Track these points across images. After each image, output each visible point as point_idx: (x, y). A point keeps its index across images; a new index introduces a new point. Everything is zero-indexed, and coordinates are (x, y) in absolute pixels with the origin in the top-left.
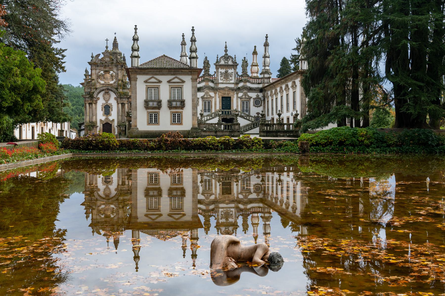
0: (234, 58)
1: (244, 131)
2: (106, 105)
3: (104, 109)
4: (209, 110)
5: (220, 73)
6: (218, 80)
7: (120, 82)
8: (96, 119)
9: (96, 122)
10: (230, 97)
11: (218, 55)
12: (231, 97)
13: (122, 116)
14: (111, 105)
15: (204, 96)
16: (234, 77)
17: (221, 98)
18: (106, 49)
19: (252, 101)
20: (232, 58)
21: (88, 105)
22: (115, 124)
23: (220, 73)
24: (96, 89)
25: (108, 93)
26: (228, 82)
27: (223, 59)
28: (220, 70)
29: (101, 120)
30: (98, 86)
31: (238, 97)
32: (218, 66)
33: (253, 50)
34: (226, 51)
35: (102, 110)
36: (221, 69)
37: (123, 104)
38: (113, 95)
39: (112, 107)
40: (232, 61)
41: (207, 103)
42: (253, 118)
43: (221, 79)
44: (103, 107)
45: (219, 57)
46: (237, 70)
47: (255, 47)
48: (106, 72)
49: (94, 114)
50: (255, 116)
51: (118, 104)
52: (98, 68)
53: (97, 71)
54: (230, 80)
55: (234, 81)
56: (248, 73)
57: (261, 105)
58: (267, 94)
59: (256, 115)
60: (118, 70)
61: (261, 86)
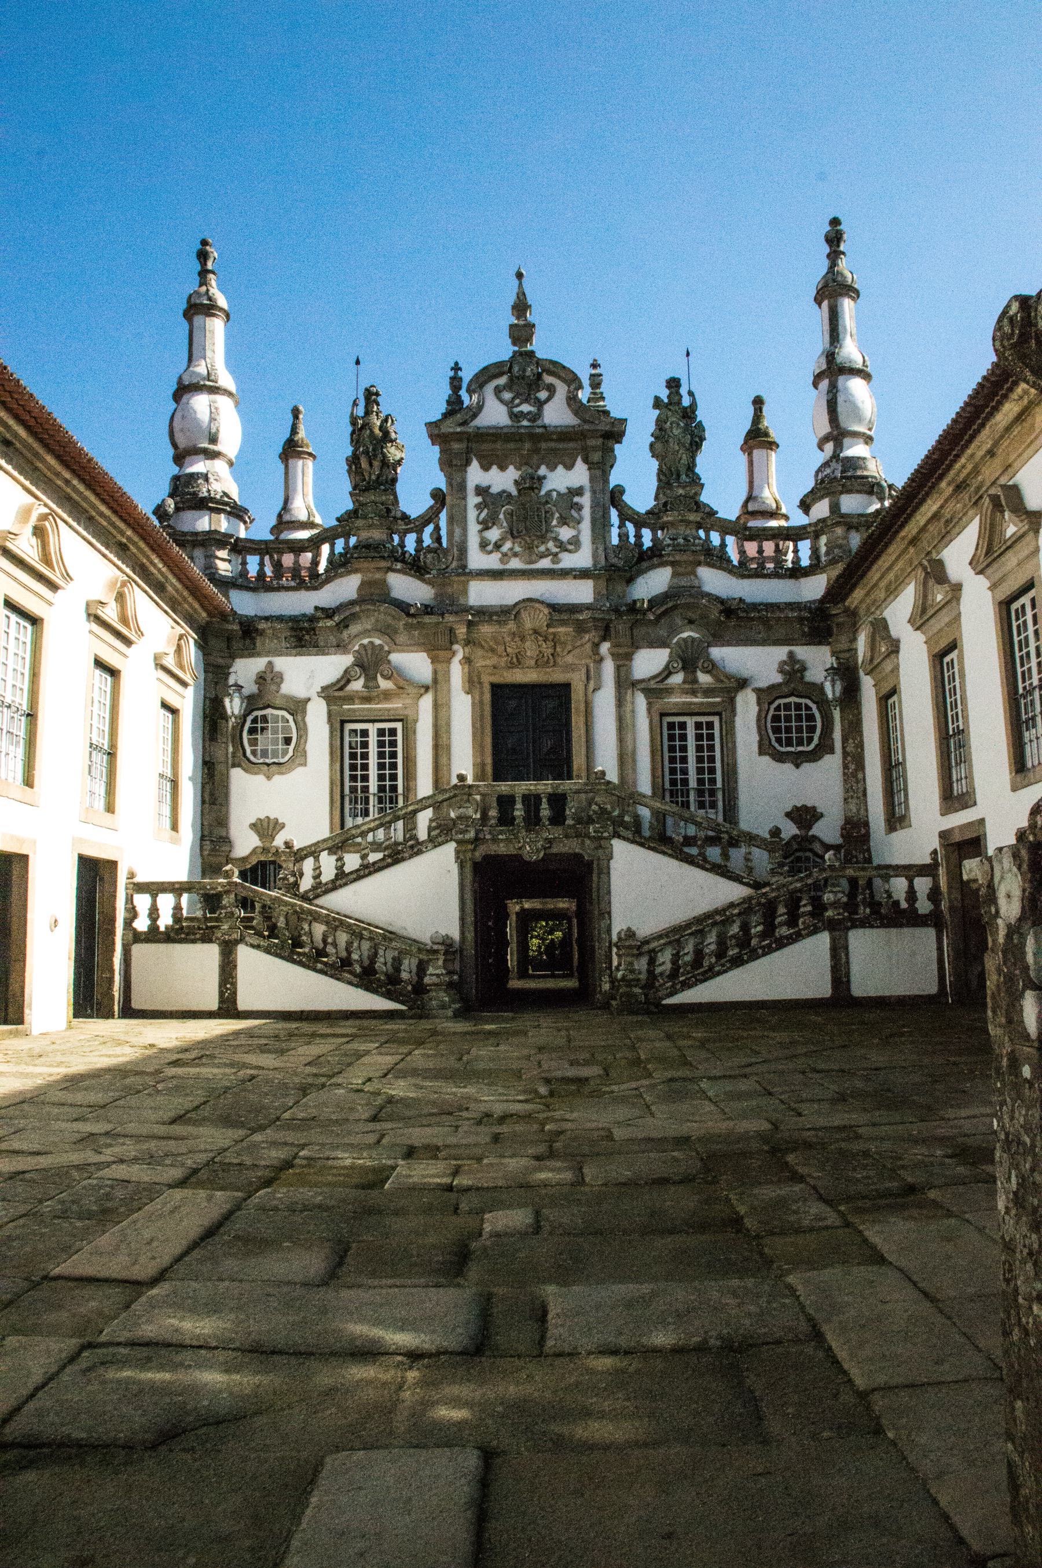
0: (584, 374)
1: (674, 974)
4: (388, 793)
5: (473, 500)
6: (463, 551)
10: (565, 688)
11: (456, 368)
12: (567, 686)
15: (346, 678)
16: (594, 522)
17: (487, 697)
19: (747, 707)
20: (572, 380)
23: (473, 500)
26: (545, 563)
27: (498, 391)
28: (475, 475)
31: (625, 684)
32: (456, 446)
33: (747, 425)
34: (521, 333)
36: (486, 468)
40: (572, 400)
41: (373, 740)
42: (761, 859)
43: (483, 545)
45: (467, 375)
46: (614, 479)
47: (758, 402)
50: (776, 832)
54: (562, 547)
55: (595, 555)
56: (704, 498)
57: (825, 748)
58: (881, 627)
59: (789, 830)
61: (814, 588)
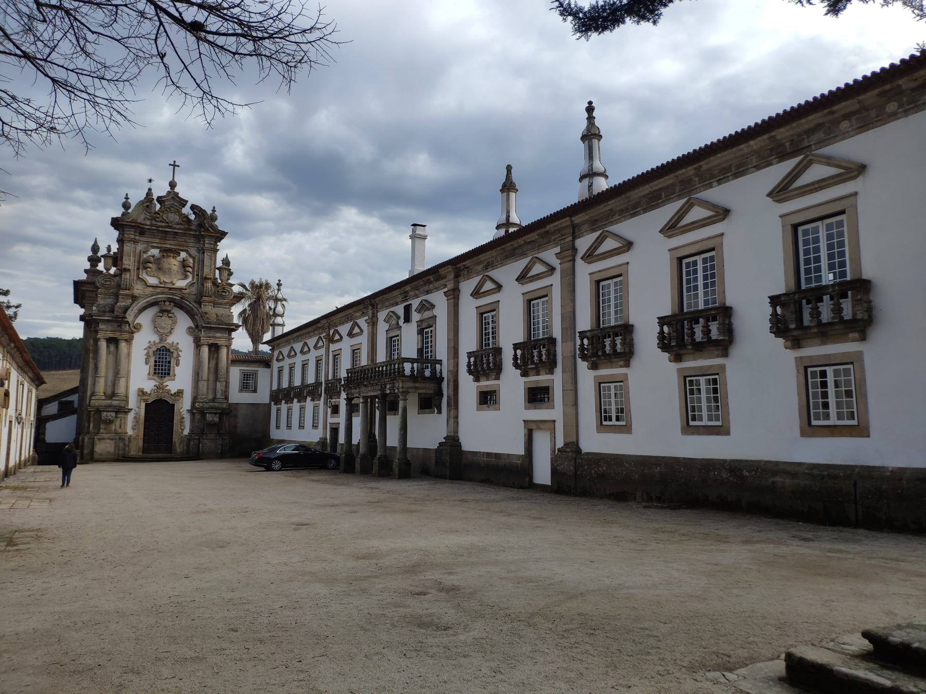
2: (160, 346)
3: (152, 360)
7: (209, 284)
8: (127, 387)
9: (127, 396)
13: (208, 380)
14: (177, 349)
18: (168, 189)
21: (103, 344)
22: (184, 405)
24: (134, 298)
25: (168, 312)
29: (142, 392)
30: (138, 289)
35: (147, 363)
37: (214, 348)
38: (183, 322)
39: (178, 354)
44: (151, 354)
48: (166, 252)
49: (123, 371)
51: (198, 344)
52: (142, 239)
53: (140, 247)
60: (202, 251)
